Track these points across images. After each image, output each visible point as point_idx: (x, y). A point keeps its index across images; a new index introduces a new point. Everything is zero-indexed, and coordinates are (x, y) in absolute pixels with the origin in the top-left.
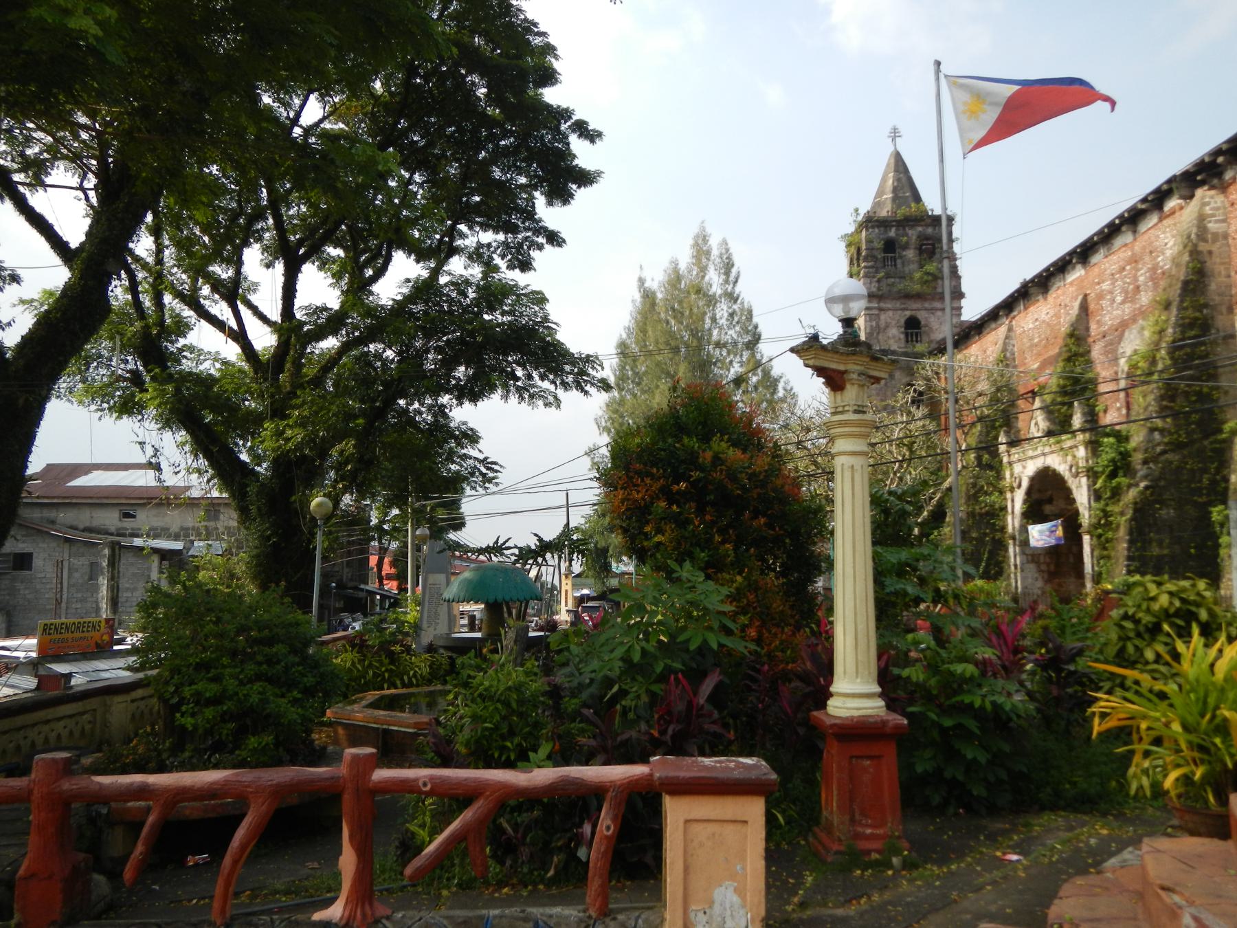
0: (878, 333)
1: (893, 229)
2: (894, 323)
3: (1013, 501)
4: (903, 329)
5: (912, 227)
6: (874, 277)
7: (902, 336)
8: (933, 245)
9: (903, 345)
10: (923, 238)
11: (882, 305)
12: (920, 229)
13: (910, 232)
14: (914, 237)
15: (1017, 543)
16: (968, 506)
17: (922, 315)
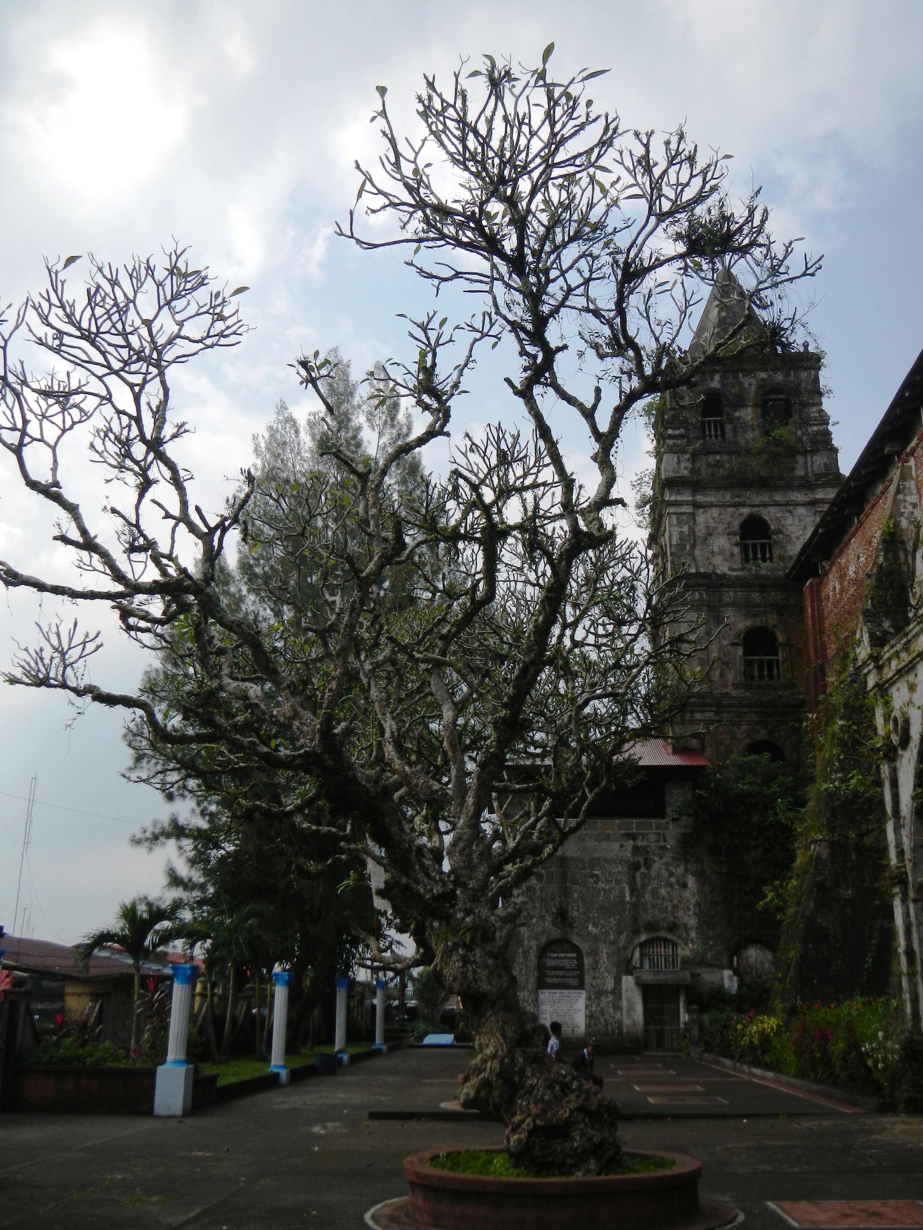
0: (693, 546)
1: (717, 377)
2: (721, 527)
3: (895, 783)
4: (738, 538)
5: (748, 373)
6: (684, 452)
7: (736, 550)
8: (787, 401)
9: (738, 565)
10: (767, 391)
11: (700, 498)
12: (763, 375)
13: (746, 381)
14: (753, 388)
15: (911, 894)
16: (832, 830)
17: (771, 515)
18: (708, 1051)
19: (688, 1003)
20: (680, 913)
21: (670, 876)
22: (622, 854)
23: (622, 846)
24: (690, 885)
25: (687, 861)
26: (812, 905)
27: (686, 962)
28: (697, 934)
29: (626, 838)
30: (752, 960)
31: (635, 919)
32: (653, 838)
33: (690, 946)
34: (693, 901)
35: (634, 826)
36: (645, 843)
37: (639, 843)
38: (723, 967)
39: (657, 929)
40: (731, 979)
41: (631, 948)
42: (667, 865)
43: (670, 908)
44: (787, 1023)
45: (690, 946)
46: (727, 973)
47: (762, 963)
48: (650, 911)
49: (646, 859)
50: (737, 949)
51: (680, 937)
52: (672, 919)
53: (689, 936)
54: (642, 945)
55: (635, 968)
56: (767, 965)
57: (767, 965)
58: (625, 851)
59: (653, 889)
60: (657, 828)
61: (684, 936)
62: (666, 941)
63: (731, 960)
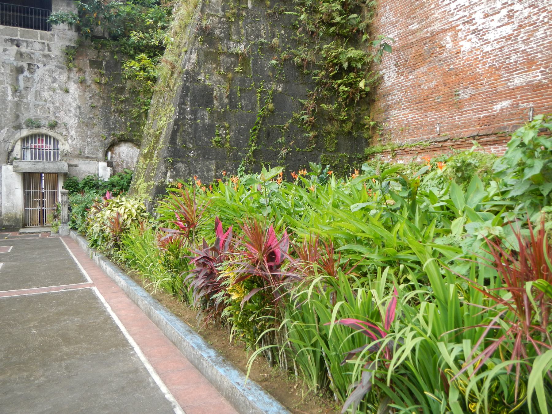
18: (74, 229)
19: (66, 187)
20: (62, 114)
21: (53, 82)
22: (6, 57)
23: (5, 50)
24: (71, 91)
25: (70, 70)
26: (194, 57)
27: (66, 155)
28: (77, 132)
29: (9, 43)
30: (123, 156)
31: (17, 117)
32: (37, 46)
33: (70, 141)
34: (74, 105)
35: (19, 33)
36: (29, 50)
37: (23, 49)
38: (98, 160)
39: (39, 127)
40: (105, 170)
41: (12, 141)
42: (51, 71)
43: (51, 109)
44: (152, 205)
45: (70, 141)
46: (102, 165)
48: (33, 110)
49: (29, 65)
50: (111, 146)
51: (61, 134)
52: (53, 119)
53: (69, 133)
54: (25, 140)
55: (16, 159)
58: (9, 55)
59: (36, 91)
60: (42, 38)
61: (64, 133)
62: (47, 136)
63: (106, 154)
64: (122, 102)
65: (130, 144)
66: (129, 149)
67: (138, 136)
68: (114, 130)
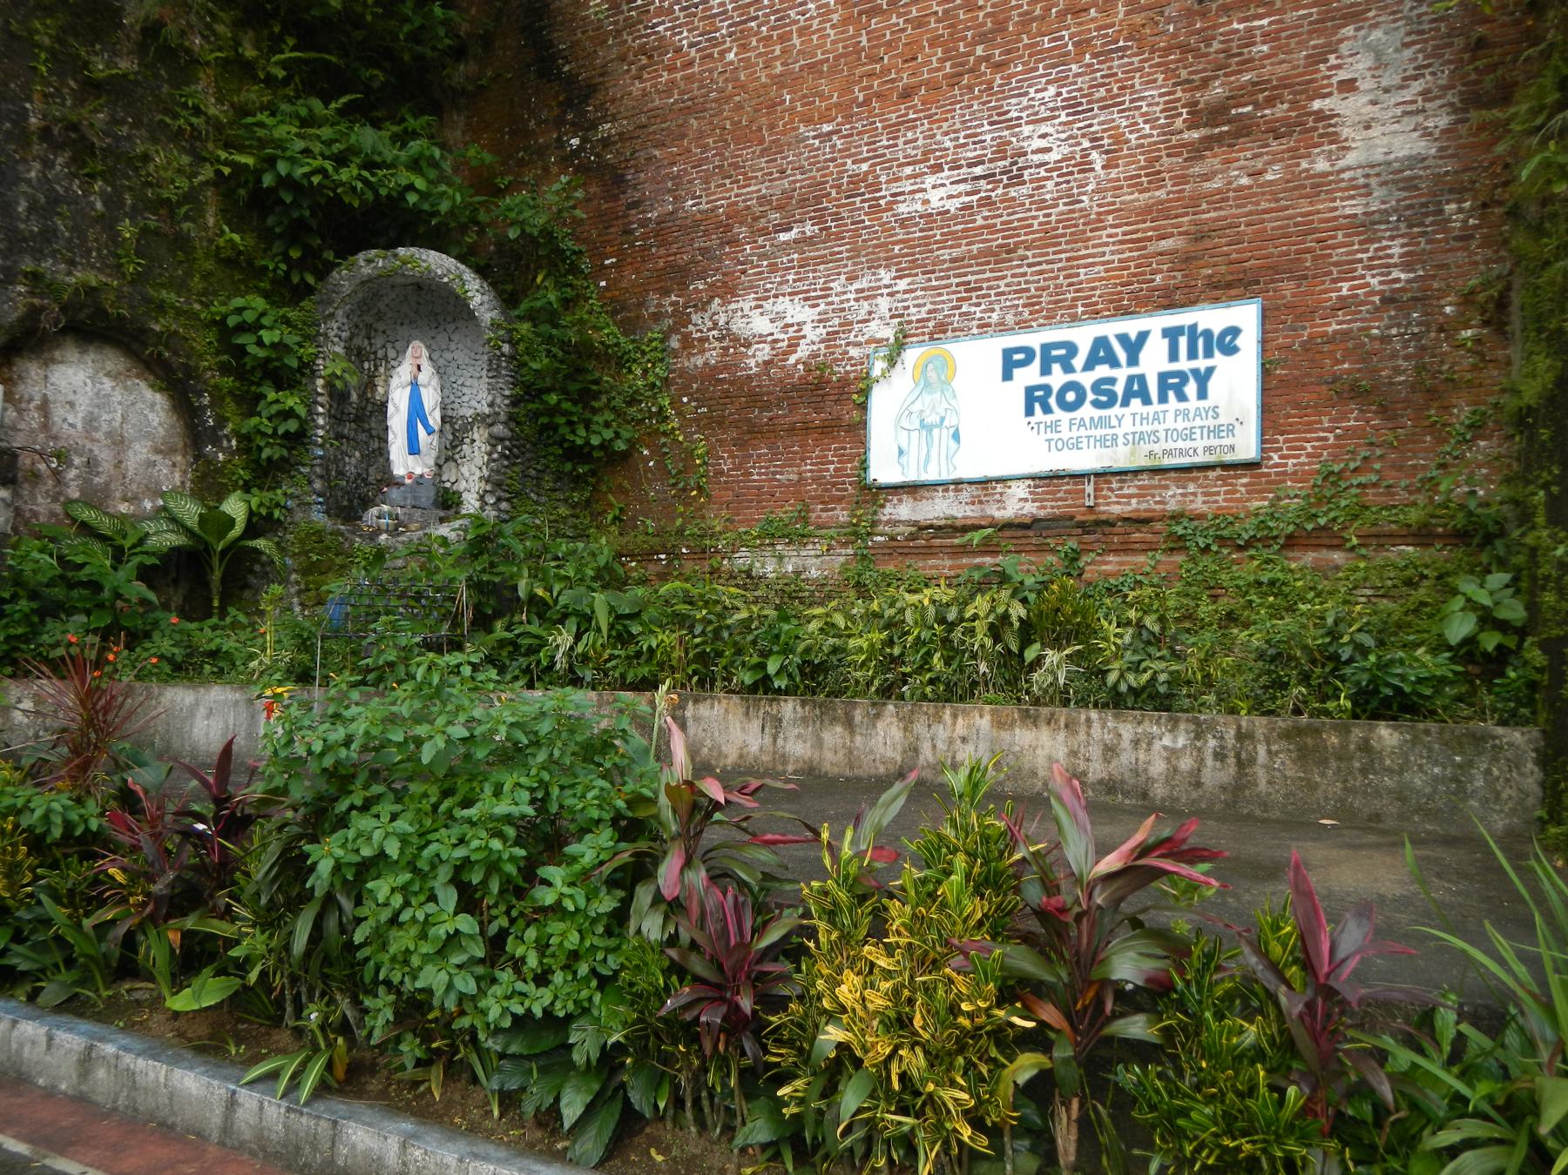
30: (70, 422)
47: (119, 442)
56: (138, 453)
57: (138, 453)
64: (93, 88)
65: (114, 361)
66: (108, 384)
67: (179, 312)
68: (38, 255)
